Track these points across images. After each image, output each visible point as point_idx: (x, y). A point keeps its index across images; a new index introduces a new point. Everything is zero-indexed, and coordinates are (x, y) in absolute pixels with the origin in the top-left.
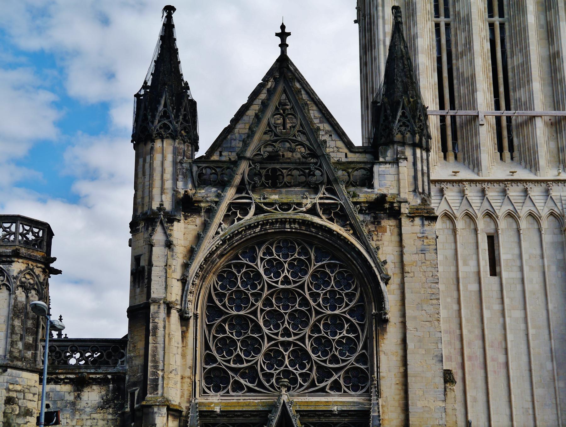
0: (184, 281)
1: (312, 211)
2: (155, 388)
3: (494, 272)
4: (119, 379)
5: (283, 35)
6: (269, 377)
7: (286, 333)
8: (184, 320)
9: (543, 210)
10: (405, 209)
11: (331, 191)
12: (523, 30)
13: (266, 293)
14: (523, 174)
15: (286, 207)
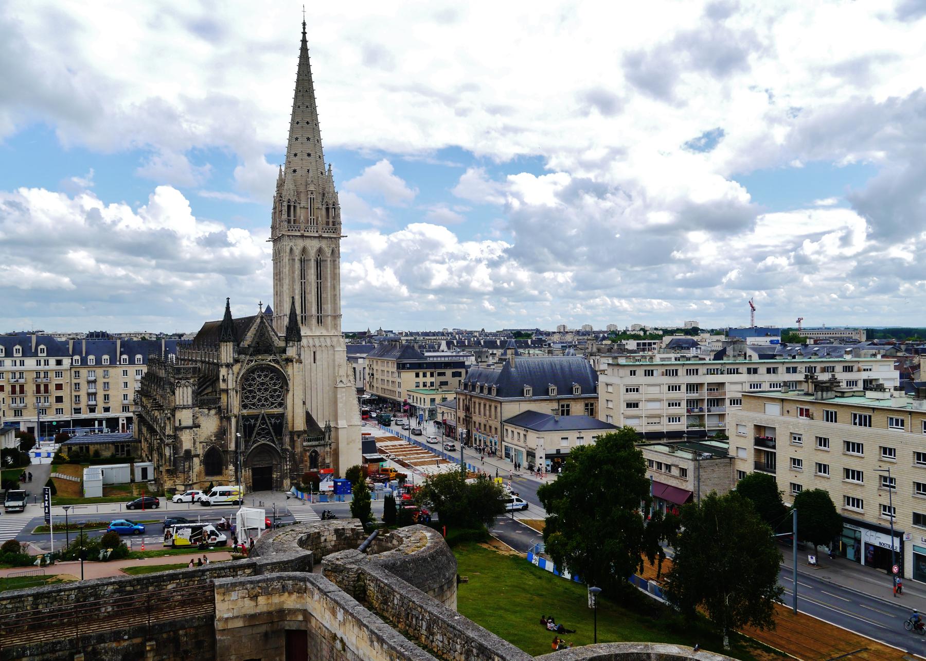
0: (236, 382)
1: (270, 361)
2: (231, 412)
3: (315, 363)
4: (220, 407)
5: (261, 305)
6: (258, 405)
7: (263, 393)
8: (237, 392)
9: (329, 344)
10: (294, 360)
11: (275, 355)
12: (327, 287)
13: (257, 383)
14: (325, 333)
15: (263, 360)
